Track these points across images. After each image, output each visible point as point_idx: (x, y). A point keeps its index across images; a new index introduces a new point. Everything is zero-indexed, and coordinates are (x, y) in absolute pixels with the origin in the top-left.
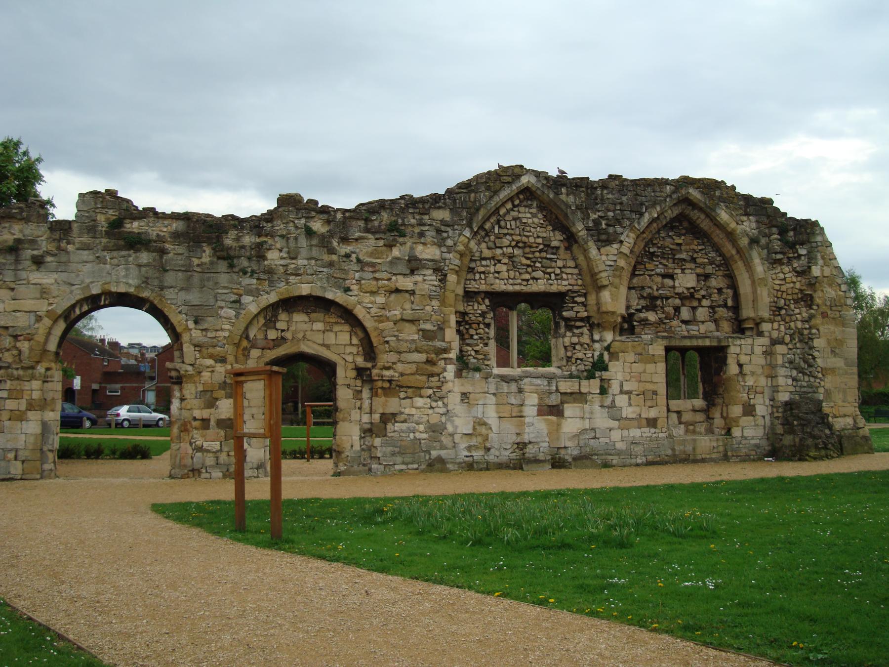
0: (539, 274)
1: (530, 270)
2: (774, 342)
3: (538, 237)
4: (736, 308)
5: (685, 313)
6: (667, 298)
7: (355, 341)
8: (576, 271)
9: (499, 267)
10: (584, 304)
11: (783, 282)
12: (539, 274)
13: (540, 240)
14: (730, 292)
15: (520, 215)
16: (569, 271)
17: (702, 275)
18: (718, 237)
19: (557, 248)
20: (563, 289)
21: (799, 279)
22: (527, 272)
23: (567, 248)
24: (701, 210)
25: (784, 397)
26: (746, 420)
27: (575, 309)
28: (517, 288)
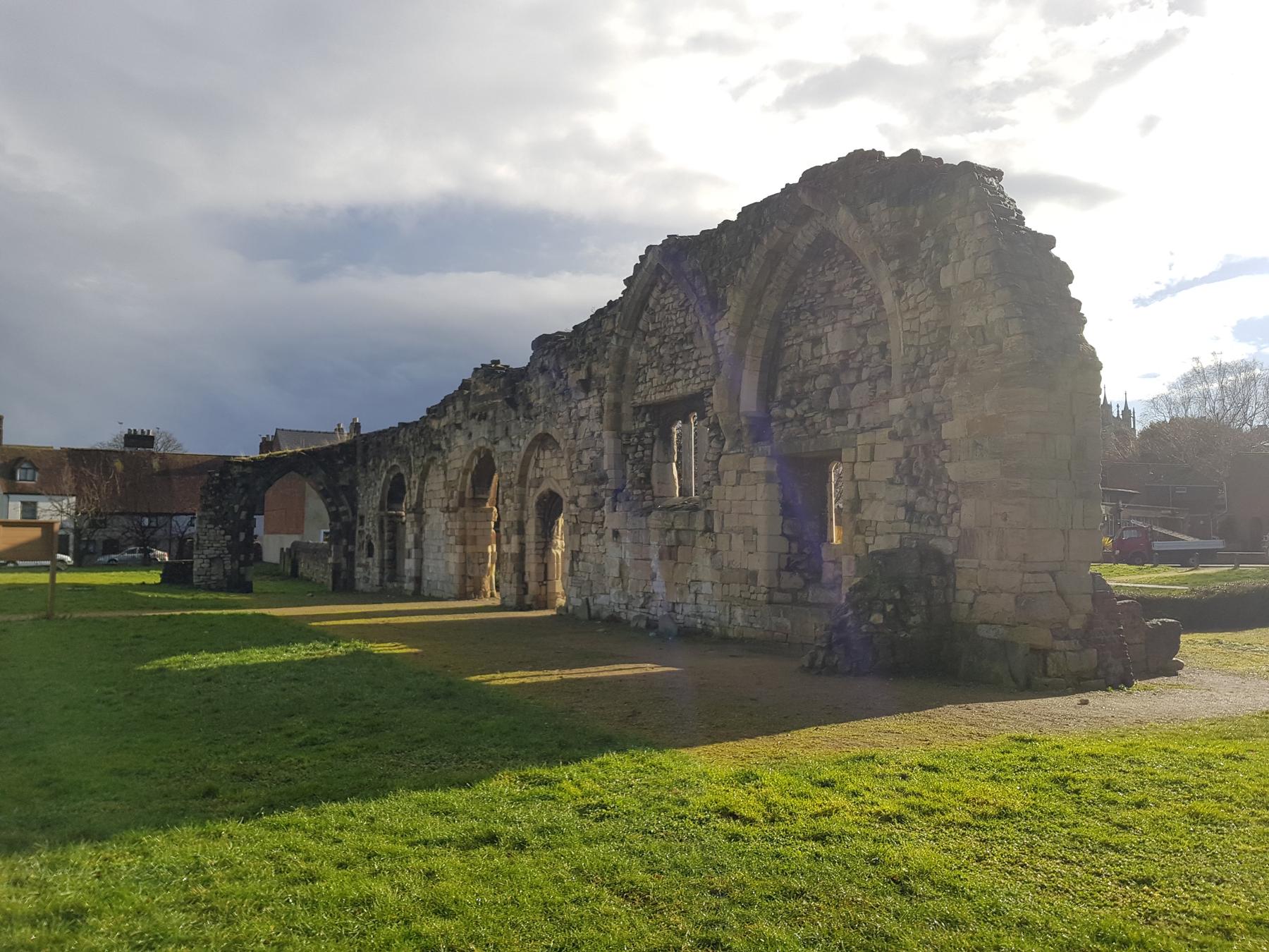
3: (678, 325)
5: (834, 402)
12: (679, 374)
13: (678, 329)
20: (697, 388)
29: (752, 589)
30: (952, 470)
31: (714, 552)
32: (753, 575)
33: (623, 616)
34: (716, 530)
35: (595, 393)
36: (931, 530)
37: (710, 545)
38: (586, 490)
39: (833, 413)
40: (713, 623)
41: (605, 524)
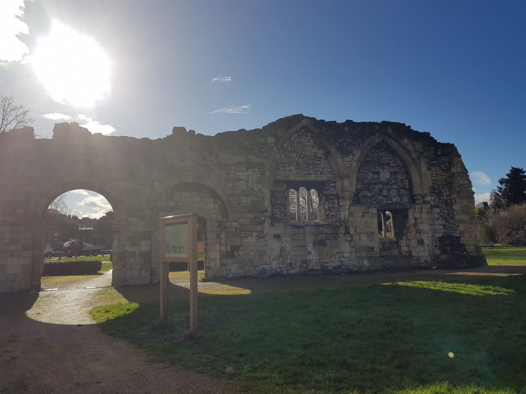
0: (312, 171)
1: (307, 169)
2: (432, 207)
4: (411, 190)
5: (385, 193)
6: (376, 184)
7: (217, 207)
8: (330, 170)
9: (291, 167)
10: (334, 187)
11: (436, 176)
12: (312, 171)
14: (407, 182)
15: (302, 141)
16: (327, 170)
17: (393, 172)
18: (401, 152)
19: (321, 158)
20: (324, 179)
21: (445, 174)
22: (305, 170)
23: (326, 158)
24: (393, 138)
25: (438, 235)
26: (420, 248)
27: (330, 190)
28: (301, 178)
29: (373, 253)
30: (457, 217)
31: (350, 241)
32: (372, 248)
33: (285, 272)
34: (352, 232)
35: (256, 170)
36: (452, 231)
37: (349, 239)
38: (251, 215)
39: (384, 196)
40: (352, 267)
41: (265, 232)
